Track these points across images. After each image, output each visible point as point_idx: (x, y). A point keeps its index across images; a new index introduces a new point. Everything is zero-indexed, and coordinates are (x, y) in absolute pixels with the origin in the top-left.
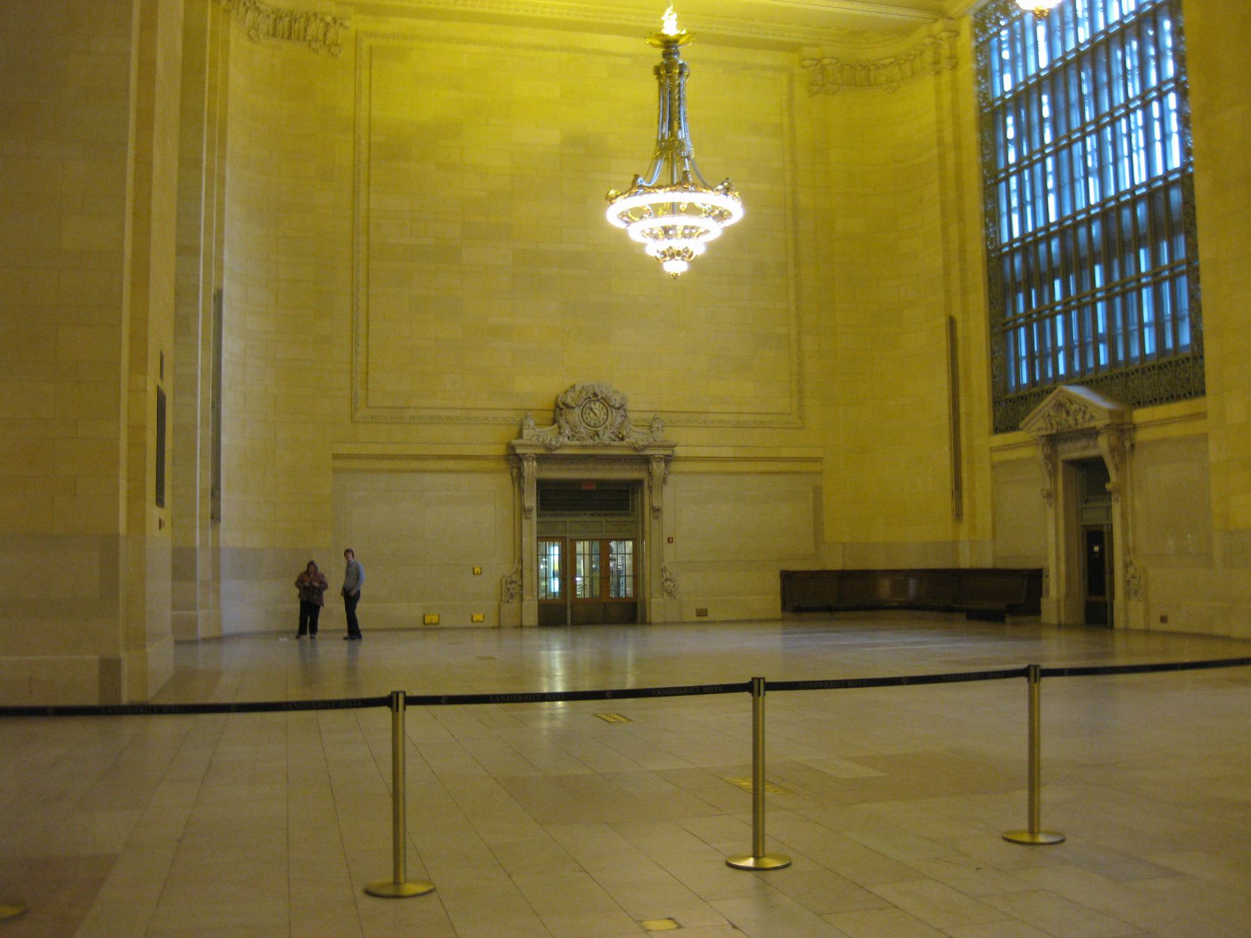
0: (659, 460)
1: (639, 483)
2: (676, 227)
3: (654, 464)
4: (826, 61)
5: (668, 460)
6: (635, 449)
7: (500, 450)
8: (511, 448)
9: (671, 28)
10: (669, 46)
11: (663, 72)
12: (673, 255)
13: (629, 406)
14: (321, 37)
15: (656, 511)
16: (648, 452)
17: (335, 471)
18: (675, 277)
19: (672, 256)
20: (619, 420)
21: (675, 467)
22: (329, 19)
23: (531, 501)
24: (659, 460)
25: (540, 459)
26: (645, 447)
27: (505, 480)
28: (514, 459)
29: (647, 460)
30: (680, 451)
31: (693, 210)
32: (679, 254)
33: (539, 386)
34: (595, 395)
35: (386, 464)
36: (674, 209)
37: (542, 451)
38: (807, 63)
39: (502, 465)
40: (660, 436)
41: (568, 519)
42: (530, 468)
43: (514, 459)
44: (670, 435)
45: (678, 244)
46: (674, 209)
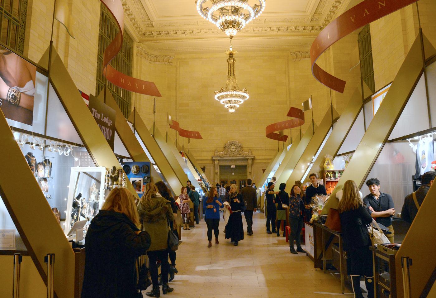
1: (247, 165)
4: (296, 53)
5: (253, 160)
7: (210, 158)
8: (212, 157)
9: (231, 49)
10: (231, 55)
13: (243, 146)
15: (250, 173)
16: (247, 158)
18: (232, 113)
20: (240, 150)
21: (256, 161)
23: (218, 170)
25: (219, 160)
29: (247, 160)
30: (257, 157)
31: (236, 96)
32: (233, 107)
34: (233, 143)
36: (232, 96)
37: (219, 158)
38: (292, 53)
39: (211, 162)
40: (250, 153)
42: (216, 162)
44: (255, 153)
45: (233, 105)
46: (232, 96)
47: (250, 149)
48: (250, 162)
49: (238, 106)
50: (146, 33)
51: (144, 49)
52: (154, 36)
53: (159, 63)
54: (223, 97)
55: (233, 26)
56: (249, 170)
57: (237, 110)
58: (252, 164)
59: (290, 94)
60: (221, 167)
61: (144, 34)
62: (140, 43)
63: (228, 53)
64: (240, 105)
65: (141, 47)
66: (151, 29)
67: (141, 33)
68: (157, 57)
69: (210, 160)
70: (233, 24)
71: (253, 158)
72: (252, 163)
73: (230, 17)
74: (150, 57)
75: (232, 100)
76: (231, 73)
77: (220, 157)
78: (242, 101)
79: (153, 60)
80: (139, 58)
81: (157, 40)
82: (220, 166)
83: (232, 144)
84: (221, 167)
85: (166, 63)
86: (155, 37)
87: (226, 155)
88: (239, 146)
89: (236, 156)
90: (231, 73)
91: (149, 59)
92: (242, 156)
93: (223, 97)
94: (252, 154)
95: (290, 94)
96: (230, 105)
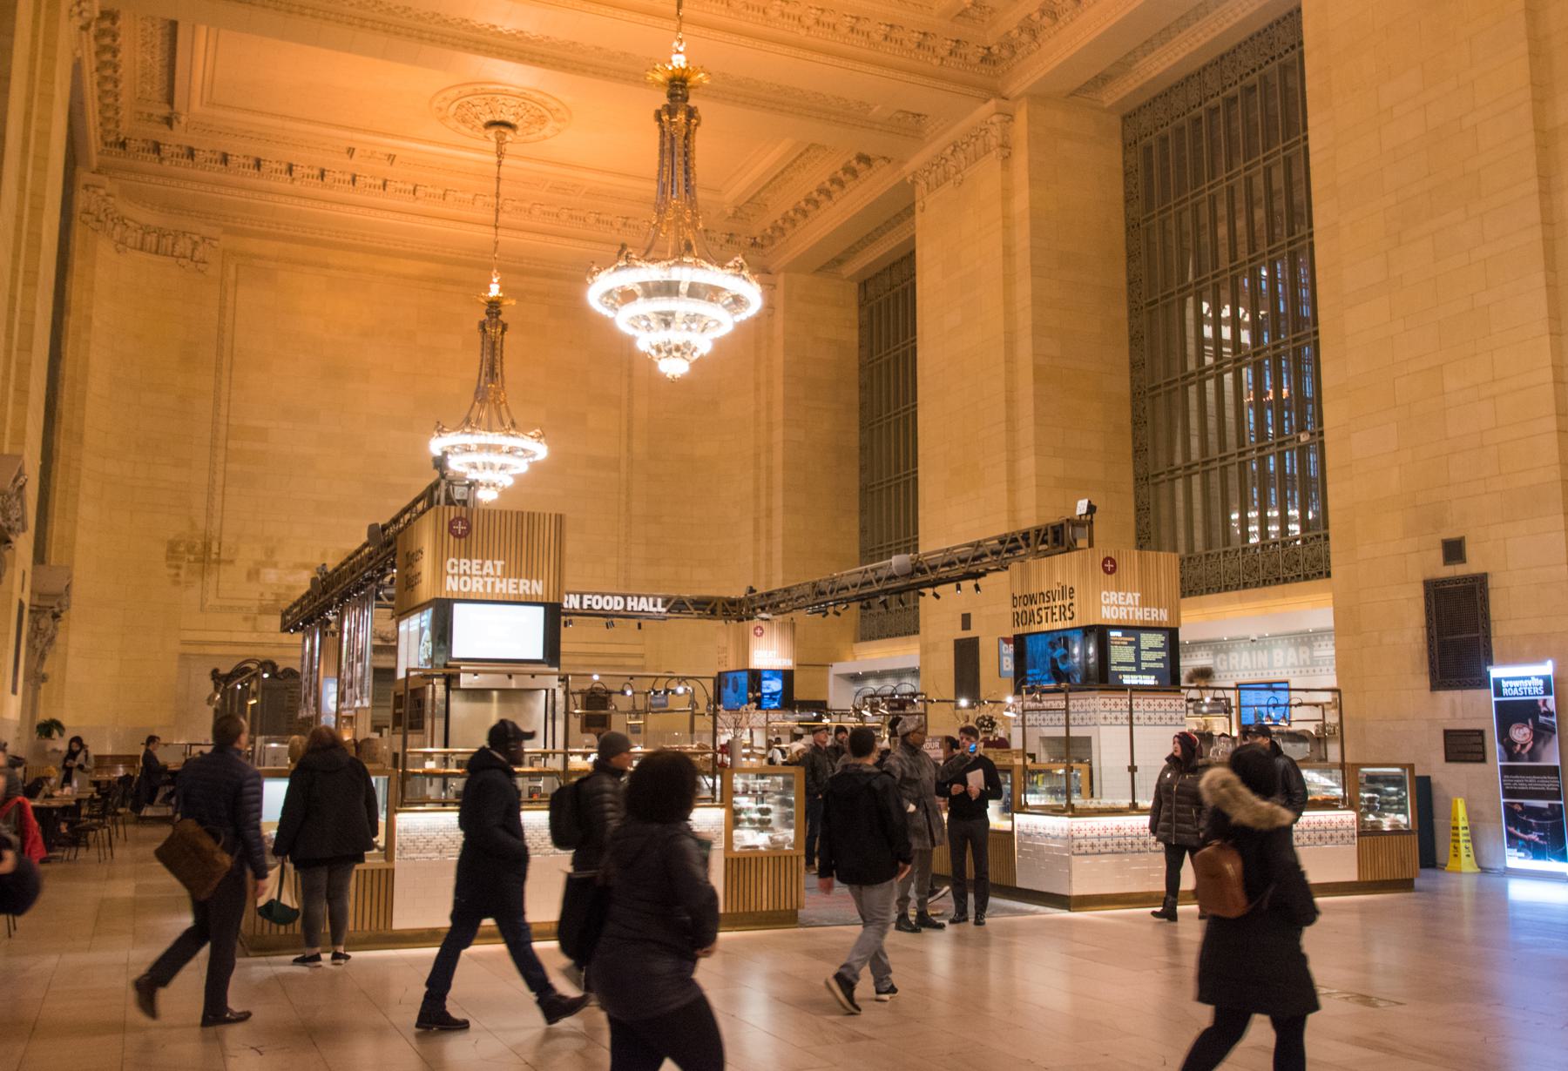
10: (494, 307)
14: (188, 253)
22: (196, 238)
36: (490, 448)
46: (490, 448)
52: (161, 160)
53: (155, 258)
59: (630, 436)
61: (123, 145)
62: (97, 177)
68: (146, 230)
74: (118, 229)
77: (382, 639)
79: (130, 241)
81: (171, 177)
85: (181, 261)
91: (116, 237)
95: (630, 436)
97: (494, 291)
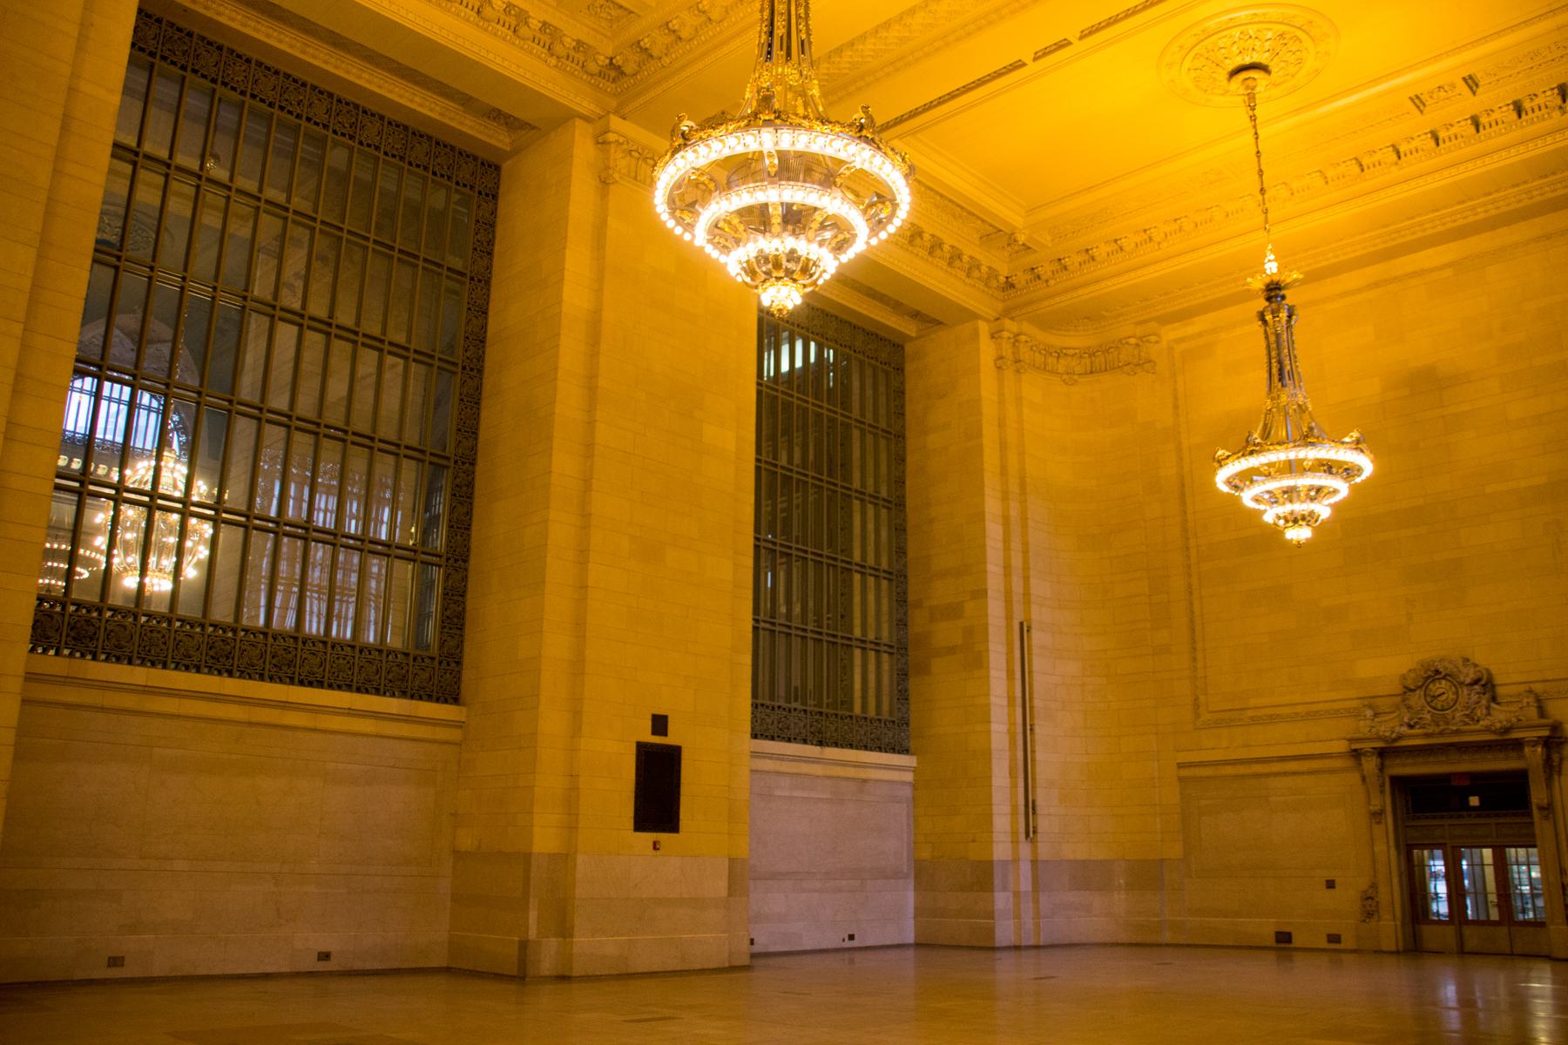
0: (1534, 743)
2: (1296, 490)
3: (1527, 750)
6: (1494, 732)
7: (1341, 747)
10: (1274, 291)
11: (1268, 317)
12: (1295, 520)
13: (1498, 680)
16: (1515, 735)
17: (1181, 779)
18: (1299, 545)
19: (1295, 521)
20: (1475, 698)
24: (1534, 743)
25: (1382, 753)
26: (1508, 730)
27: (1355, 778)
28: (1356, 754)
29: (1518, 745)
32: (1303, 518)
33: (1385, 668)
34: (1437, 672)
35: (1229, 770)
36: (1292, 468)
39: (1348, 763)
41: (1447, 822)
43: (1356, 754)
46: (1292, 468)
47: (1530, 691)
48: (1534, 756)
49: (1323, 511)
50: (1013, 280)
51: (1023, 338)
54: (1248, 477)
55: (789, 273)
56: (1537, 796)
57: (1322, 529)
58: (1551, 768)
60: (1401, 785)
63: (1258, 284)
64: (1335, 507)
65: (1006, 334)
66: (1029, 260)
67: (994, 283)
69: (1339, 755)
70: (790, 266)
71: (1546, 733)
72: (1548, 760)
73: (776, 243)
75: (1296, 490)
76: (1281, 371)
78: (1342, 488)
80: (1009, 374)
82: (1397, 781)
83: (1434, 674)
84: (1401, 785)
86: (1052, 282)
87: (1411, 727)
88: (1468, 681)
89: (1458, 732)
90: (1281, 371)
92: (1488, 730)
93: (1248, 477)
94: (1542, 713)
96: (1288, 507)
97: (1272, 267)
